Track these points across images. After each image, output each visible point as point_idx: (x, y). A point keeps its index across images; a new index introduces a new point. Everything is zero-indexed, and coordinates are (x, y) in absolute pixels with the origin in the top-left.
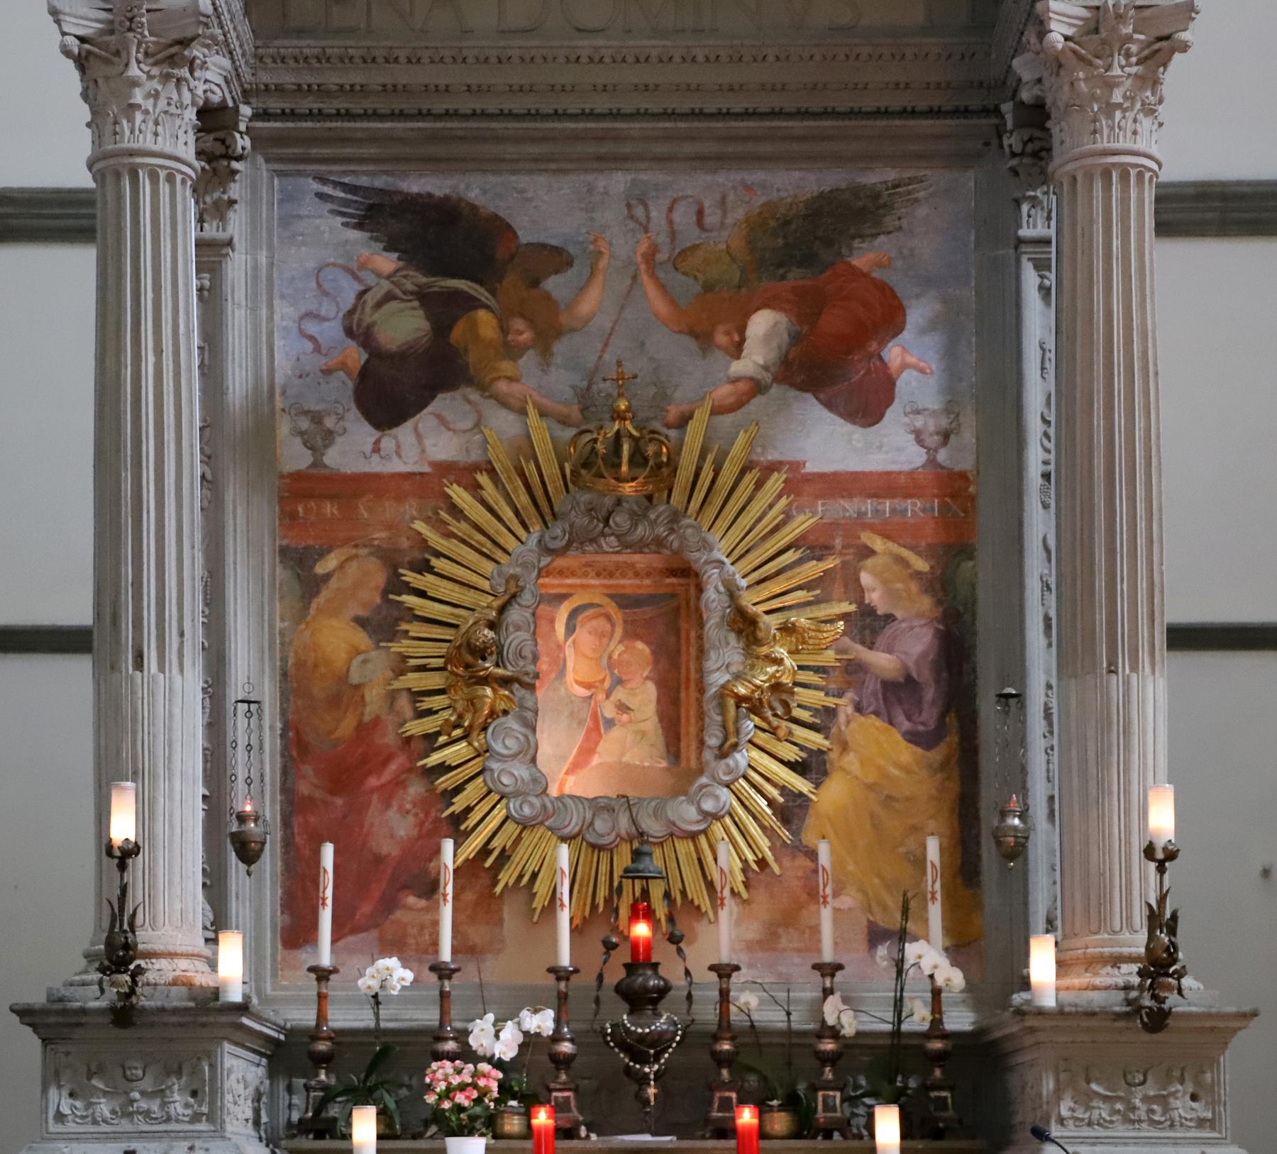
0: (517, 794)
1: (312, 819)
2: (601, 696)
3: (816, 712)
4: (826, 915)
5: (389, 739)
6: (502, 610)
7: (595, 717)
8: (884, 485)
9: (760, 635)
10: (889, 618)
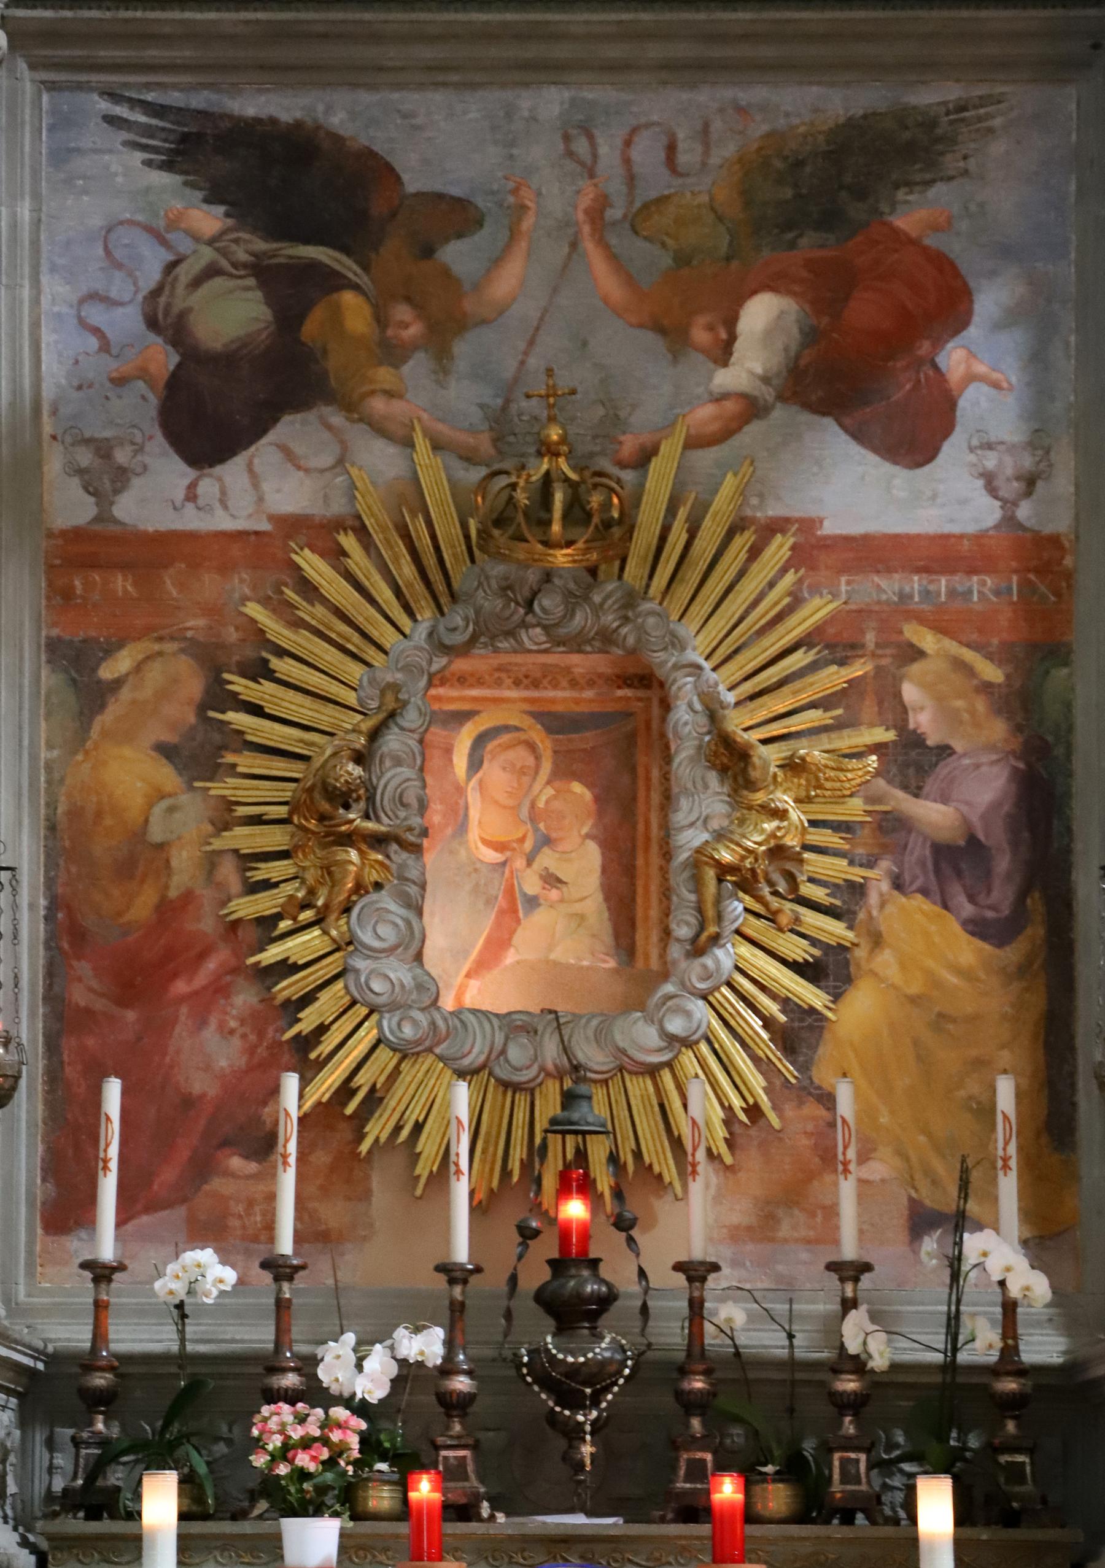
0: (393, 1007)
1: (90, 1042)
2: (519, 863)
3: (835, 888)
4: (847, 1189)
5: (207, 925)
6: (374, 735)
7: (510, 892)
9: (754, 774)
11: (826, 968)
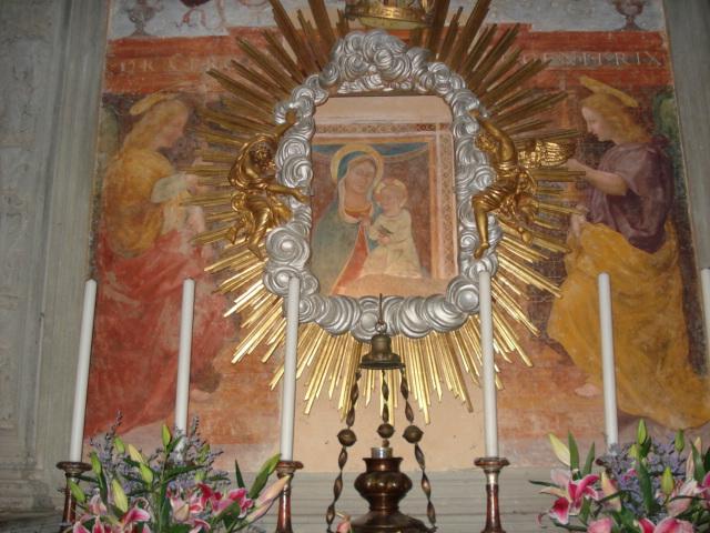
10: (609, 144)
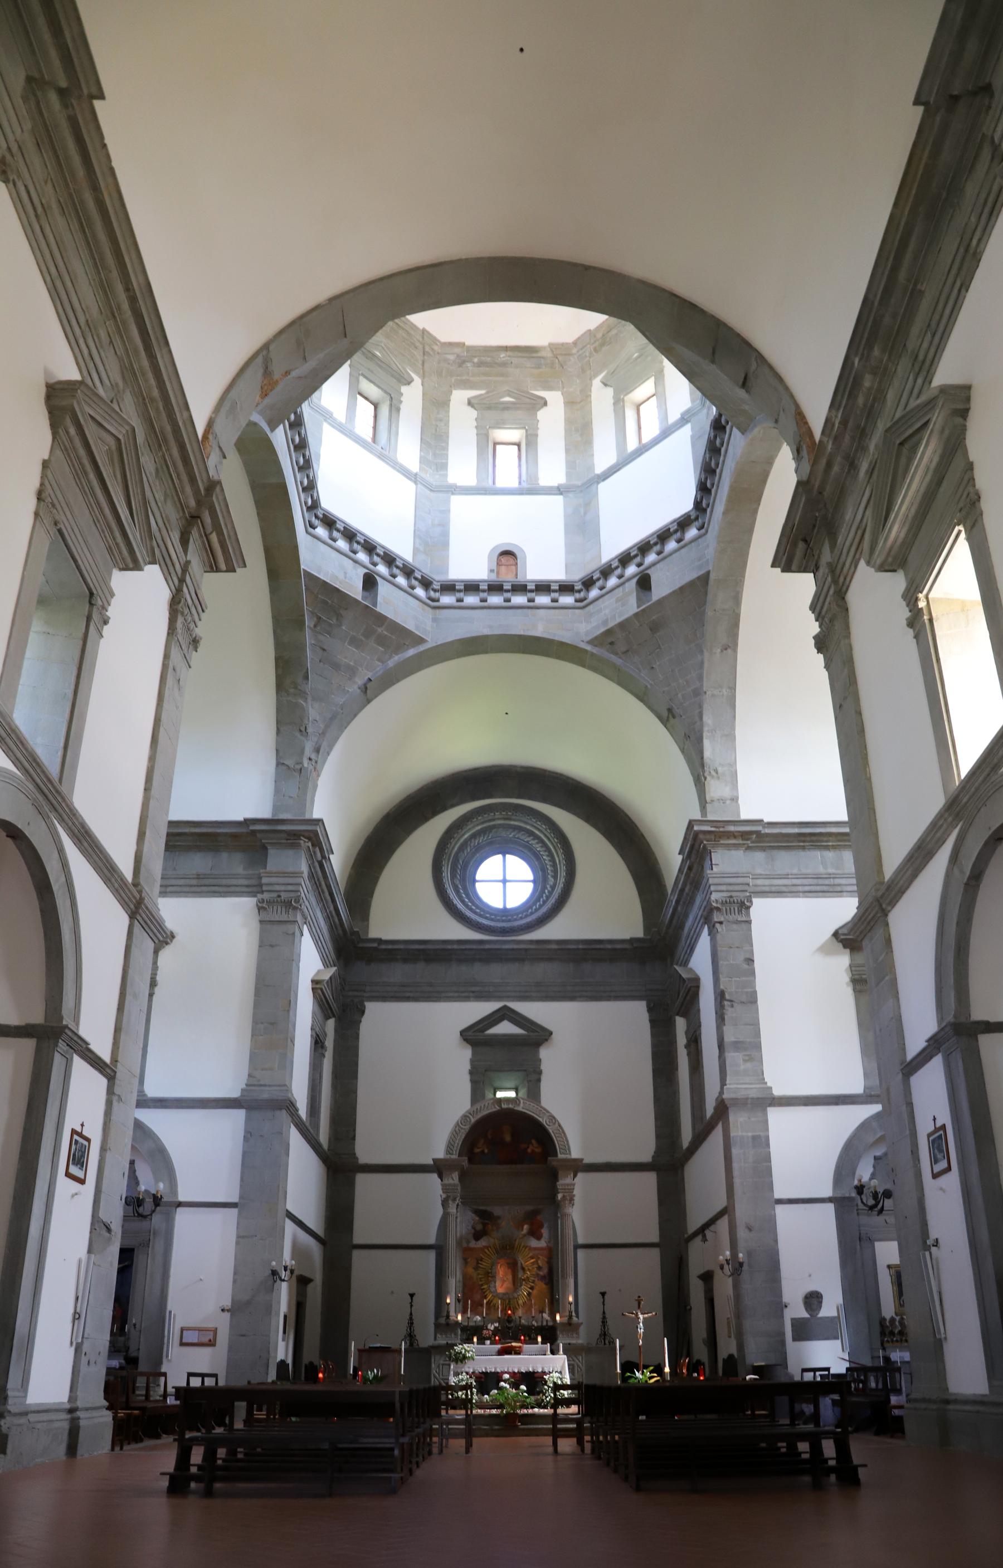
8: (541, 1249)
11: (532, 1288)
